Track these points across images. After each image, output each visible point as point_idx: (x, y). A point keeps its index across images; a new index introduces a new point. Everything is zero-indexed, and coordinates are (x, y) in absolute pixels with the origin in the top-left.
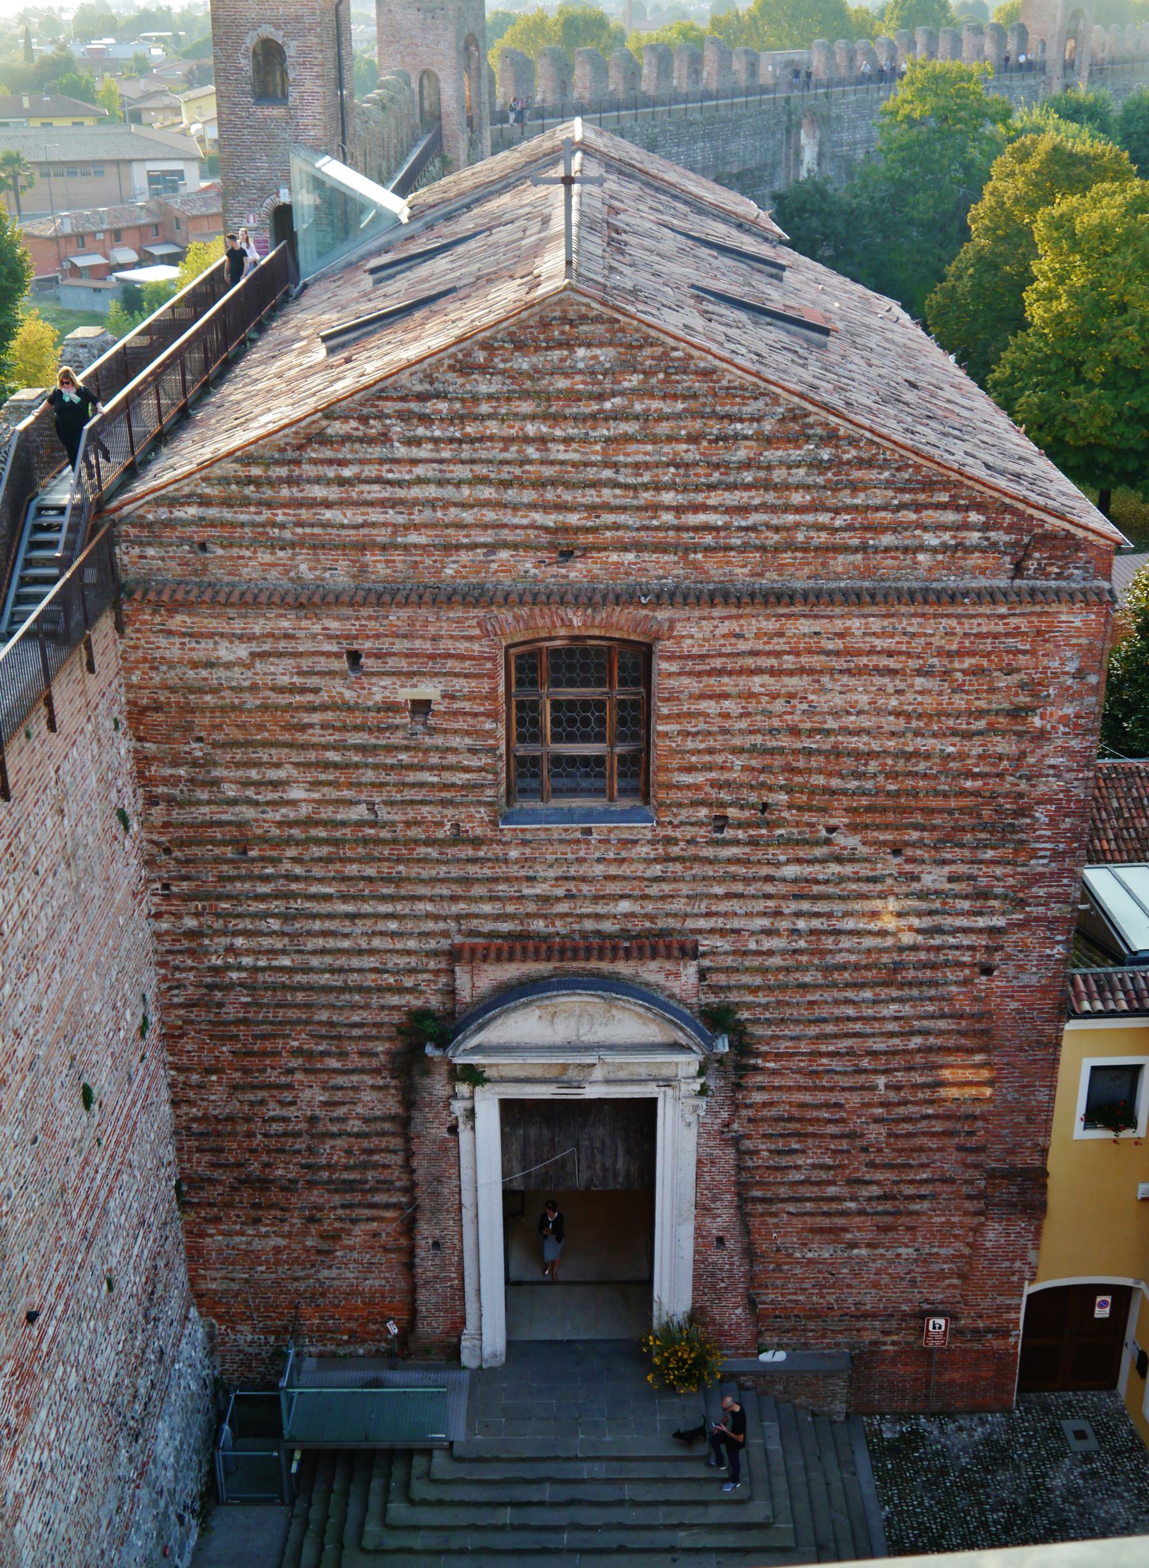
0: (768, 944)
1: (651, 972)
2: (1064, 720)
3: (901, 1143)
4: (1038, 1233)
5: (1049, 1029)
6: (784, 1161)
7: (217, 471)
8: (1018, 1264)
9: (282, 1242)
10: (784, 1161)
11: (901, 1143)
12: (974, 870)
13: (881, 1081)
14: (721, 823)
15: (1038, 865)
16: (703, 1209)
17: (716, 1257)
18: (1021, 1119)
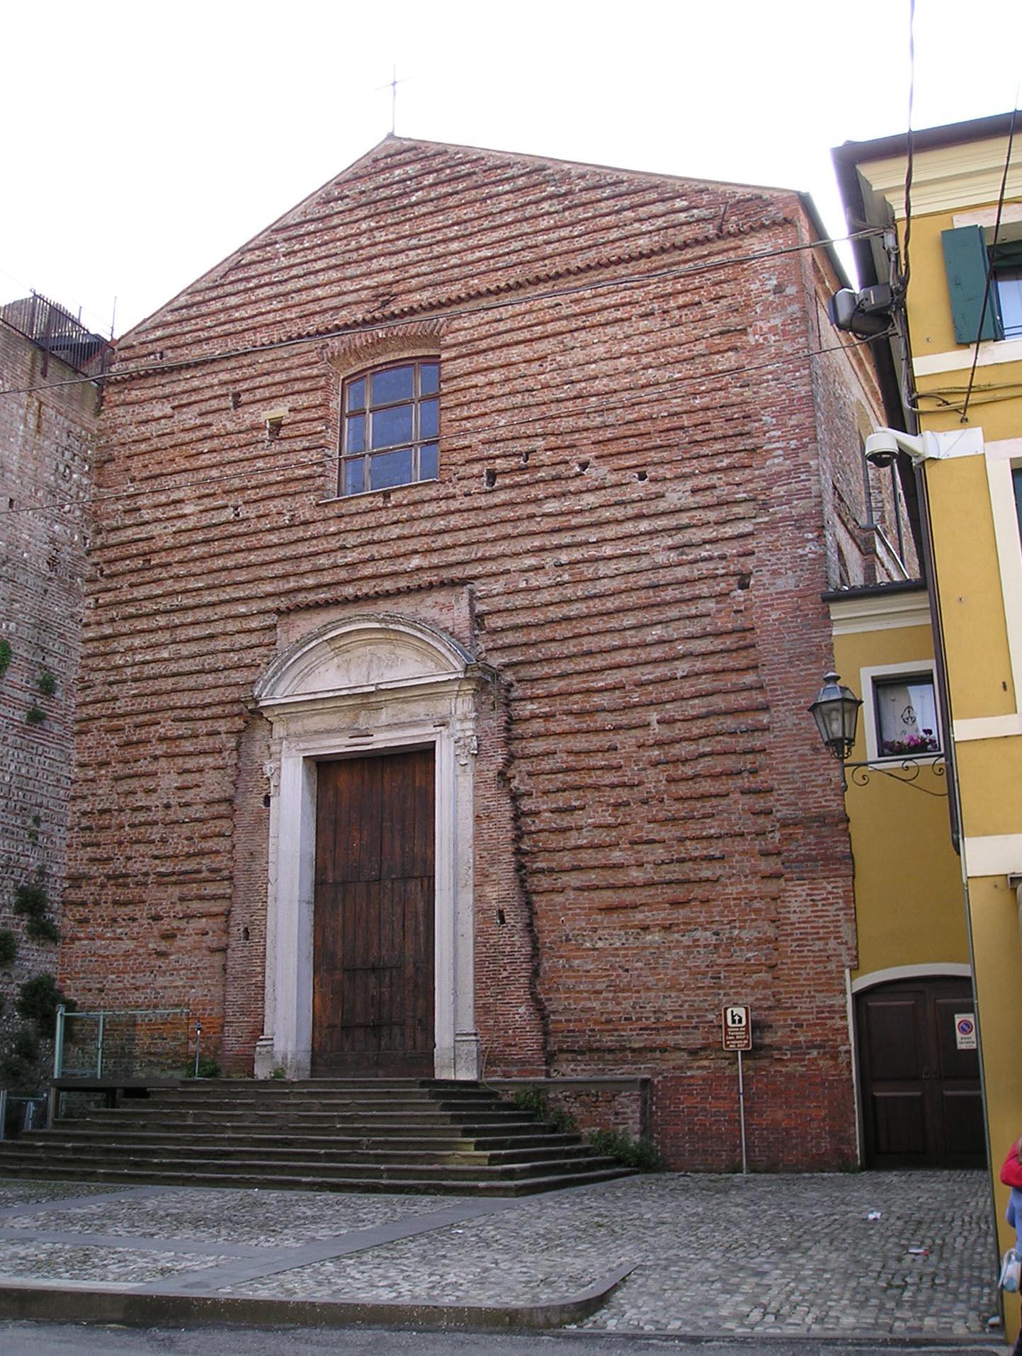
0: (537, 580)
1: (428, 607)
2: (773, 329)
3: (683, 789)
4: (850, 900)
5: (816, 637)
6: (566, 821)
7: (176, 305)
8: (832, 943)
9: (130, 945)
10: (566, 821)
11: (683, 789)
12: (714, 479)
13: (654, 717)
14: (492, 476)
15: (776, 463)
16: (482, 877)
17: (499, 936)
18: (806, 750)
